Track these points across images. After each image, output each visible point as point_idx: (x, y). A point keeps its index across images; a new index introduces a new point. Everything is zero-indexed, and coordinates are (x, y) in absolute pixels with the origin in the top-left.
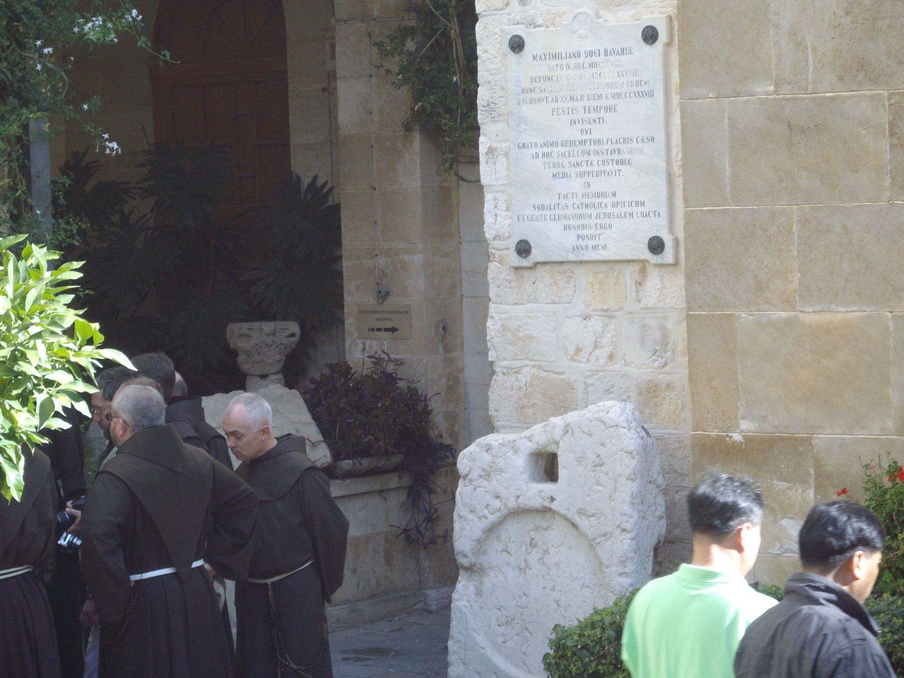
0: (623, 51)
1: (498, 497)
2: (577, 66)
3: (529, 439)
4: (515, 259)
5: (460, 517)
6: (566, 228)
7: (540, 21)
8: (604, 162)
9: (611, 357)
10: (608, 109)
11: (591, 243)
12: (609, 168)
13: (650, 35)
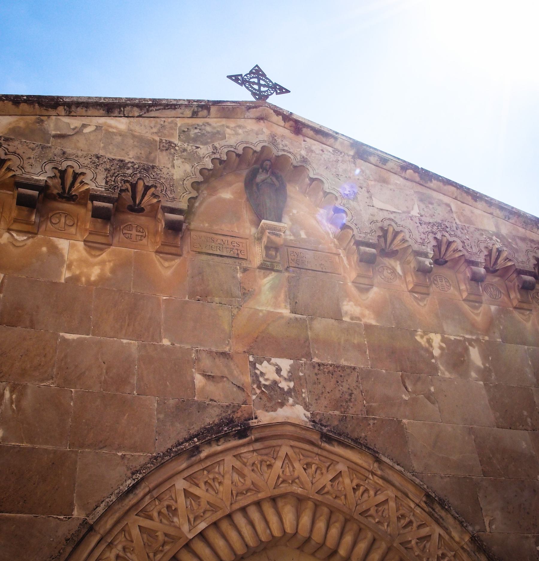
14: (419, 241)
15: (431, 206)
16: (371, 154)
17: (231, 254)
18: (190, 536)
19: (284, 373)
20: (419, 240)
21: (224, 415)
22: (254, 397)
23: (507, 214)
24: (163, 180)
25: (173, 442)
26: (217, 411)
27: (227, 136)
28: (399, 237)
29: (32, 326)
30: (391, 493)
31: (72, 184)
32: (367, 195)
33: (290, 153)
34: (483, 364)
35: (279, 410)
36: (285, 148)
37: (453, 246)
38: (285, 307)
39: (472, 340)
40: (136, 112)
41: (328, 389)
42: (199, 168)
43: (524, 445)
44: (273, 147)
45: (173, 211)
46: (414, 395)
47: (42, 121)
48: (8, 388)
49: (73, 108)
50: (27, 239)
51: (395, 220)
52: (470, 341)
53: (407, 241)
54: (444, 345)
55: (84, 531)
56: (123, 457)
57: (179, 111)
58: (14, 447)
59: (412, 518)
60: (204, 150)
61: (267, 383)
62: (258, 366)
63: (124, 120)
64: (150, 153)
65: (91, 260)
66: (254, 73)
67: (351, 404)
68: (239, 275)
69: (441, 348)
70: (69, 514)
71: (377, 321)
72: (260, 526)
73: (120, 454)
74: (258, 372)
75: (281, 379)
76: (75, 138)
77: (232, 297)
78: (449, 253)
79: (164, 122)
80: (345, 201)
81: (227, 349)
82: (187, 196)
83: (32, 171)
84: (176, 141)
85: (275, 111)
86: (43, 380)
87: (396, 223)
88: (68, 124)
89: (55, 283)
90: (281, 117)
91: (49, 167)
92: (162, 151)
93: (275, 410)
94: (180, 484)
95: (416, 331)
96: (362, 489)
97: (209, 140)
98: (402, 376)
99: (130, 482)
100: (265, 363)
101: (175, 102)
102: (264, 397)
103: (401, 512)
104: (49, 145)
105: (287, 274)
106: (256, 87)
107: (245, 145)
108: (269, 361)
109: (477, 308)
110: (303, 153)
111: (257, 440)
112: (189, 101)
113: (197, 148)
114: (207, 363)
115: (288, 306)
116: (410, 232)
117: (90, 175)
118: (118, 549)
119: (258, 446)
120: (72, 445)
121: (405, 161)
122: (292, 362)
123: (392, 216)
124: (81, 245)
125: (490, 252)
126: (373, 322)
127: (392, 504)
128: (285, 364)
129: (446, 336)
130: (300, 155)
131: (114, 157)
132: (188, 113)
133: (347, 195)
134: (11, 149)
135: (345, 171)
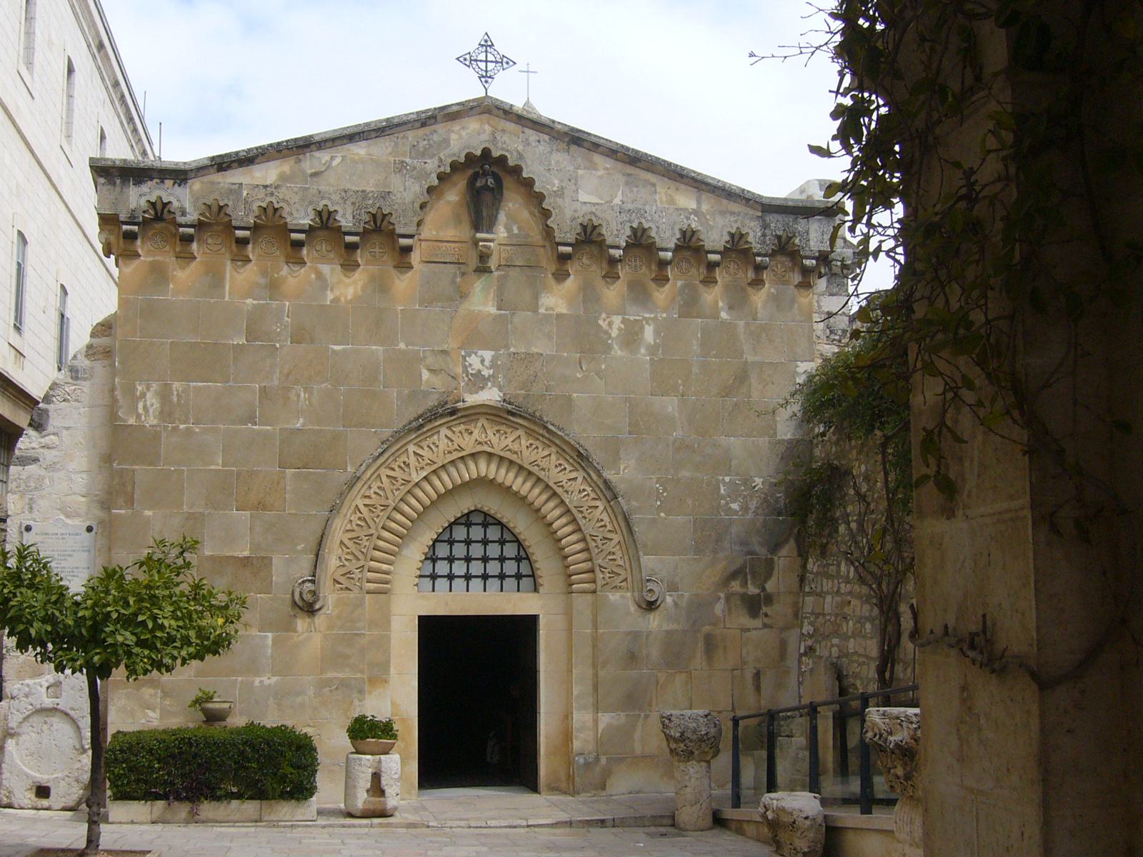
0: (77, 534)
1: (31, 705)
2: (58, 538)
3: (47, 681)
10: (69, 555)
14: (616, 232)
15: (635, 189)
16: (584, 140)
17: (454, 260)
18: (417, 481)
19: (487, 363)
22: (462, 384)
24: (396, 207)
25: (405, 422)
26: (436, 396)
27: (452, 142)
28: (597, 231)
30: (554, 449)
31: (328, 219)
33: (507, 151)
34: (654, 340)
35: (480, 392)
36: (504, 146)
39: (650, 318)
40: (373, 134)
41: (519, 373)
42: (426, 187)
43: (670, 409)
44: (492, 148)
49: (323, 144)
51: (598, 213)
53: (603, 235)
54: (623, 326)
55: (354, 481)
58: (310, 429)
59: (567, 466)
60: (432, 166)
61: (473, 372)
63: (364, 143)
64: (386, 178)
65: (347, 280)
68: (458, 280)
69: (620, 329)
70: (345, 470)
71: (568, 310)
74: (467, 364)
75: (484, 368)
76: (326, 173)
77: (452, 300)
78: (644, 238)
80: (552, 199)
81: (445, 347)
82: (416, 220)
83: (298, 216)
84: (408, 160)
86: (322, 383)
87: (596, 216)
89: (322, 306)
91: (310, 209)
93: (478, 393)
94: (412, 448)
95: (600, 314)
96: (534, 446)
99: (380, 450)
100: (473, 355)
101: (405, 118)
102: (470, 384)
103: (559, 462)
107: (467, 151)
108: (476, 354)
109: (664, 286)
110: (520, 148)
111: (462, 417)
112: (417, 113)
113: (425, 163)
114: (430, 360)
119: (463, 420)
120: (344, 426)
121: (617, 144)
122: (493, 353)
123: (593, 209)
124: (339, 267)
125: (684, 233)
126: (565, 311)
127: (553, 457)
128: (488, 355)
130: (518, 151)
132: (418, 124)
133: (555, 192)
134: (281, 196)
135: (558, 162)
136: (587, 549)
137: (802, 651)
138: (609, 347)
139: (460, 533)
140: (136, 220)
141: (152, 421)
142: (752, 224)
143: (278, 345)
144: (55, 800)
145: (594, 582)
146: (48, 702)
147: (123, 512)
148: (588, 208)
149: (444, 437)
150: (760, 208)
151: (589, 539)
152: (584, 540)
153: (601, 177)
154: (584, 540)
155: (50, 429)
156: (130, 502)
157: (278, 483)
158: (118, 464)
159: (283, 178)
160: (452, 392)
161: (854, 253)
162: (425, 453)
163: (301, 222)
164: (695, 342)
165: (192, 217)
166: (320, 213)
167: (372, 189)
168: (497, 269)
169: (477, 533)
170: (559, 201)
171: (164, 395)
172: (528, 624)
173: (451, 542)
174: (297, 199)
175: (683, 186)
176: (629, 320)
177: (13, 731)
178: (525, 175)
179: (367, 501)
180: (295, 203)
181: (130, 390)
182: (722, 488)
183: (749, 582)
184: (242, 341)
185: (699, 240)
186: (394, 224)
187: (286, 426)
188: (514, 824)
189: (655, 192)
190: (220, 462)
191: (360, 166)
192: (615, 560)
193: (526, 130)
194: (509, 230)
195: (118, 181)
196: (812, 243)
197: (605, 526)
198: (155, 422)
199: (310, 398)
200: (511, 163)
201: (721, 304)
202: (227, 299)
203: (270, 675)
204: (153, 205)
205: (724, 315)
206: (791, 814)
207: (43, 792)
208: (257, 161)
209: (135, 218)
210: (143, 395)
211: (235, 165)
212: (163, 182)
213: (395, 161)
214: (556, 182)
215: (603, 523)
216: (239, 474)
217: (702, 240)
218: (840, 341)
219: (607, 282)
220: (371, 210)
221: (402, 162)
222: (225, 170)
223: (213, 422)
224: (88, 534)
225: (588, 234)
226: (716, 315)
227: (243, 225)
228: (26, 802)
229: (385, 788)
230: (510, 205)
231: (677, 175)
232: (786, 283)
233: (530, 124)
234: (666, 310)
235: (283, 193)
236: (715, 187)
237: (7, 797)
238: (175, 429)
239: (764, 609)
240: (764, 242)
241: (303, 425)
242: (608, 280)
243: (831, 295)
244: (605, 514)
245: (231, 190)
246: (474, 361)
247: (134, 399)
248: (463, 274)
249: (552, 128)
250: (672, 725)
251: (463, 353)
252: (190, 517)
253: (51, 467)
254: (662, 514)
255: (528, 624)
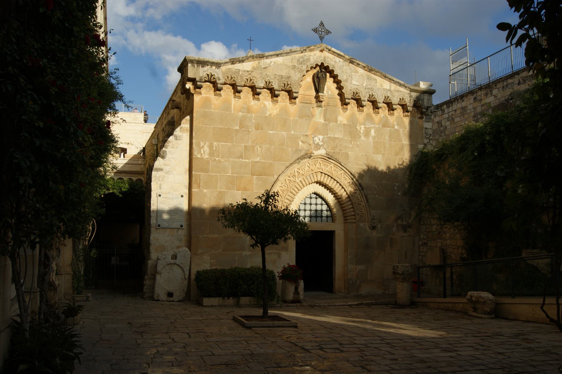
1: (166, 262)
3: (171, 253)
4: (157, 227)
5: (159, 265)
6: (167, 223)
7: (163, 192)
8: (174, 214)
9: (172, 242)
11: (171, 225)
12: (175, 214)
13: (182, 196)
14: (364, 96)
15: (370, 81)
17: (309, 102)
19: (321, 140)
20: (364, 96)
21: (306, 152)
22: (313, 147)
23: (395, 82)
24: (293, 82)
26: (304, 151)
27: (311, 60)
29: (262, 130)
30: (343, 171)
32: (351, 79)
33: (329, 64)
36: (328, 62)
37: (374, 96)
38: (323, 120)
39: (373, 127)
41: (331, 144)
45: (295, 93)
46: (353, 145)
47: (260, 62)
48: (259, 147)
49: (268, 57)
50: (258, 103)
52: (372, 127)
54: (364, 129)
56: (284, 163)
57: (297, 52)
58: (262, 162)
60: (304, 68)
62: (314, 138)
63: (281, 58)
64: (289, 71)
66: (320, 25)
67: (336, 148)
68: (311, 109)
69: (364, 130)
70: (274, 177)
72: (313, 179)
73: (283, 163)
74: (314, 140)
75: (320, 142)
79: (293, 57)
81: (307, 134)
84: (296, 65)
85: (326, 48)
88: (266, 62)
90: (328, 50)
92: (292, 69)
93: (317, 151)
94: (296, 170)
97: (306, 63)
98: (351, 140)
100: (316, 137)
101: (296, 50)
102: (315, 147)
104: (262, 72)
105: (324, 108)
106: (320, 32)
108: (317, 136)
109: (377, 115)
110: (333, 63)
113: (302, 66)
114: (302, 138)
115: (324, 119)
116: (362, 93)
117: (274, 82)
118: (284, 184)
120: (273, 161)
122: (323, 137)
126: (346, 123)
128: (321, 137)
129: (366, 126)
131: (279, 74)
132: (300, 52)
133: (345, 80)
135: (345, 69)
136: (353, 208)
137: (420, 244)
138: (360, 137)
139: (308, 201)
140: (202, 81)
141: (206, 156)
142: (407, 96)
143: (250, 130)
144: (175, 298)
145: (355, 219)
146: (172, 261)
147: (196, 190)
148: (355, 87)
149: (307, 166)
150: (409, 90)
151: (354, 204)
152: (352, 204)
153: (359, 76)
154: (352, 204)
155: (167, 158)
156: (199, 186)
157: (251, 181)
158: (194, 172)
159: (254, 69)
160: (309, 150)
161: (434, 108)
162: (301, 172)
163: (260, 85)
164: (387, 136)
165: (222, 81)
166: (266, 82)
167: (284, 75)
168: (324, 106)
169: (313, 201)
170: (346, 83)
171: (211, 147)
172: (331, 234)
173: (305, 204)
174: (259, 76)
175: (385, 81)
176: (366, 127)
177: (159, 272)
178: (335, 73)
179: (281, 188)
180: (258, 78)
181: (198, 144)
182: (395, 187)
183: (404, 220)
184: (237, 128)
185: (390, 100)
186: (291, 88)
187: (253, 160)
188: (340, 305)
189: (377, 82)
190: (231, 172)
191: (280, 66)
192: (362, 211)
193: (335, 57)
194: (328, 93)
195: (196, 66)
196: (425, 104)
197: (359, 199)
198: (207, 157)
199: (261, 150)
200: (331, 69)
201: (395, 123)
202: (232, 112)
203: (248, 251)
204: (208, 75)
205: (396, 127)
206: (484, 298)
207: (170, 295)
208: (245, 61)
209: (202, 80)
210: (203, 147)
211: (238, 62)
212: (212, 67)
213: (292, 65)
214: (345, 76)
215: (358, 199)
216: (237, 177)
217: (391, 100)
218: (429, 138)
219: (360, 113)
220: (284, 82)
221: (294, 65)
222: (234, 64)
223: (228, 157)
224: (181, 198)
225: (355, 95)
226: (394, 127)
227: (240, 85)
228: (164, 299)
229: (300, 292)
230: (328, 84)
231: (384, 77)
232: (415, 117)
233: (337, 55)
234: (378, 124)
235: (254, 74)
236: (396, 82)
237: (157, 297)
238: (215, 160)
239: (409, 230)
240: (411, 102)
241: (260, 160)
242: (360, 112)
243: (427, 122)
244: (359, 195)
245: (236, 72)
246: (316, 139)
247: (200, 148)
248: (313, 108)
249: (344, 57)
250: (399, 269)
251: (313, 136)
252: (220, 192)
253: (167, 173)
254: (377, 196)
255: (331, 234)
